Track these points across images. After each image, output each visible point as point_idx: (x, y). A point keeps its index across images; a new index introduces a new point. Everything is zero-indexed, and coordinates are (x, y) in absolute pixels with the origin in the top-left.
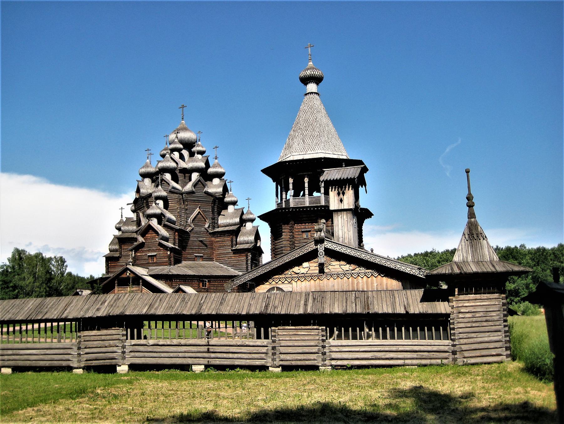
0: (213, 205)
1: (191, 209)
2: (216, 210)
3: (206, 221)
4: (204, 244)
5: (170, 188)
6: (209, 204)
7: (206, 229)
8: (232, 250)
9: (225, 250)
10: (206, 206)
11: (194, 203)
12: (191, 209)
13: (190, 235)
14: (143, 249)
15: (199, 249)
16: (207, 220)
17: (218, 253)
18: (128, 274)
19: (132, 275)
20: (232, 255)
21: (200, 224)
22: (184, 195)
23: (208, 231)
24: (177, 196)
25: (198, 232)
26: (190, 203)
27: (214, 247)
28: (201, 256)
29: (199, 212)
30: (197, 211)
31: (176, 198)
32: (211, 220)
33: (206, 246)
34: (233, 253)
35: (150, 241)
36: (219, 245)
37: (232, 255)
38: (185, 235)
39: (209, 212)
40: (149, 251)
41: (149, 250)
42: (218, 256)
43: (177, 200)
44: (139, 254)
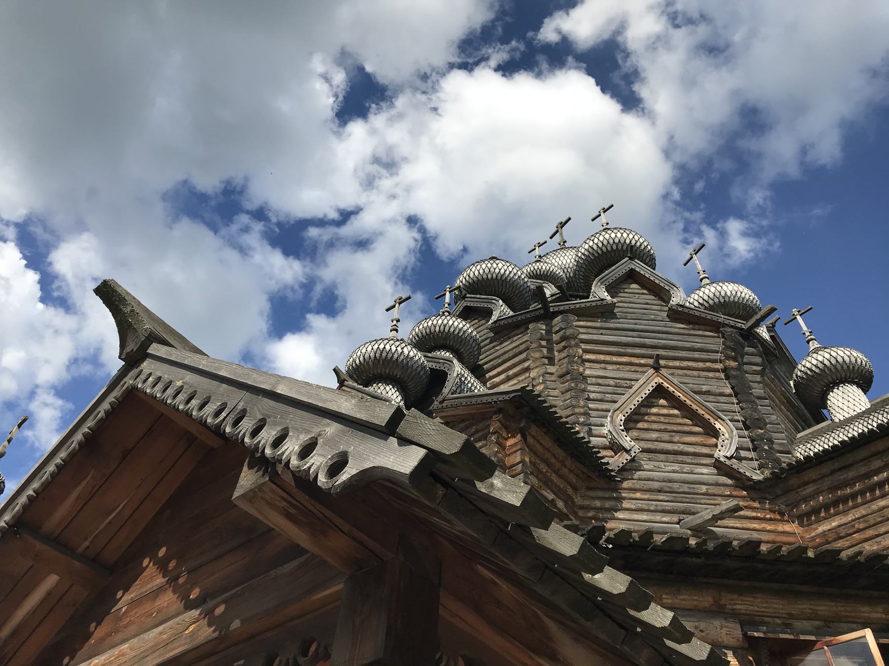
0: (733, 364)
1: (612, 382)
2: (758, 390)
3: (715, 434)
5: (494, 318)
6: (708, 364)
7: (721, 468)
10: (695, 373)
12: (612, 382)
13: (620, 499)
16: (718, 426)
21: (682, 447)
22: (559, 318)
23: (741, 481)
25: (676, 486)
26: (602, 357)
29: (659, 391)
30: (647, 382)
31: (523, 347)
32: (746, 433)
38: (594, 498)
39: (723, 399)
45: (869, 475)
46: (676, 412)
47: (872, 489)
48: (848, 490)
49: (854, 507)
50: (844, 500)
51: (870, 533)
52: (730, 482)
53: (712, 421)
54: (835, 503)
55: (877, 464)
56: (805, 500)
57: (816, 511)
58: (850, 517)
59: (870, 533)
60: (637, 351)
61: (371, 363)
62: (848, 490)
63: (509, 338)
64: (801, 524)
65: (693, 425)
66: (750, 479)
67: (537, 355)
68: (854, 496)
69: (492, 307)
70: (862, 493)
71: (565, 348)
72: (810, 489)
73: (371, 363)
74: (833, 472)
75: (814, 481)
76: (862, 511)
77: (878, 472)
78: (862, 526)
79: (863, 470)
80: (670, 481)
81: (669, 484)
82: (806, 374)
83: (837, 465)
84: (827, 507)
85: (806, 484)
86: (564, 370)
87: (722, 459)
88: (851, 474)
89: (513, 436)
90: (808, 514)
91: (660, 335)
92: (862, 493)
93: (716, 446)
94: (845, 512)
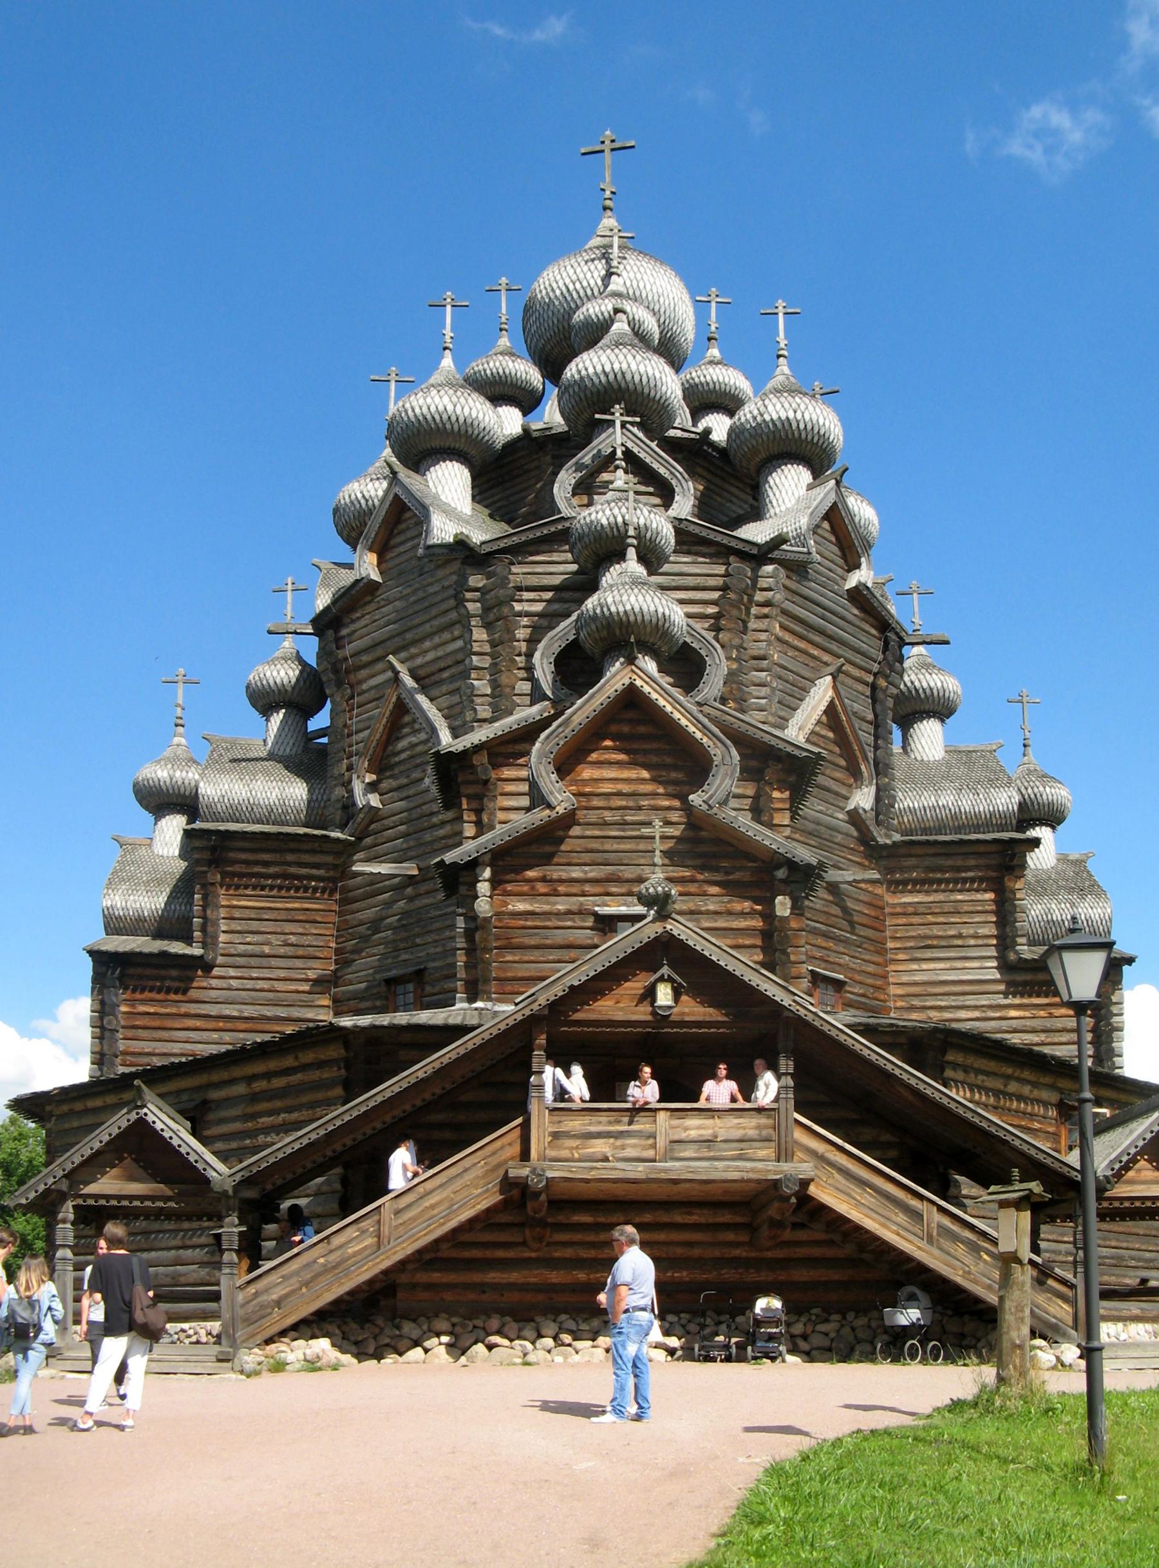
1: (791, 677)
4: (845, 910)
7: (855, 817)
8: (1005, 966)
9: (959, 964)
11: (802, 645)
12: (791, 677)
14: (556, 872)
15: (826, 936)
17: (918, 978)
18: (664, 995)
19: (692, 1010)
20: (1001, 1000)
23: (865, 838)
24: (721, 569)
25: (823, 829)
27: (890, 945)
28: (838, 985)
33: (852, 923)
34: (1009, 984)
35: (608, 816)
36: (922, 931)
37: (1001, 1000)
40: (604, 885)
41: (609, 880)
42: (916, 1002)
43: (716, 595)
44: (521, 906)
45: (959, 869)
46: (831, 735)
47: (956, 881)
48: (939, 875)
49: (936, 891)
50: (931, 882)
51: (941, 919)
52: (855, 834)
53: (860, 761)
54: (923, 882)
55: (972, 862)
56: (902, 870)
57: (905, 883)
58: (931, 899)
59: (941, 919)
60: (818, 639)
61: (648, 629)
62: (939, 875)
63: (689, 553)
64: (888, 890)
65: (841, 756)
66: (874, 839)
67: (735, 612)
68: (939, 882)
69: (677, 489)
70: (947, 881)
71: (766, 616)
72: (912, 862)
73: (648, 629)
74: (934, 855)
75: (917, 856)
76: (940, 897)
77: (968, 869)
78: (937, 910)
79: (959, 863)
80: (818, 824)
81: (818, 828)
82: (910, 692)
83: (942, 851)
84: (915, 882)
85: (911, 856)
86: (762, 652)
87: (861, 811)
88: (949, 862)
89: (779, 790)
90: (898, 883)
91: (834, 618)
92: (947, 881)
93: (851, 786)
94: (927, 892)
